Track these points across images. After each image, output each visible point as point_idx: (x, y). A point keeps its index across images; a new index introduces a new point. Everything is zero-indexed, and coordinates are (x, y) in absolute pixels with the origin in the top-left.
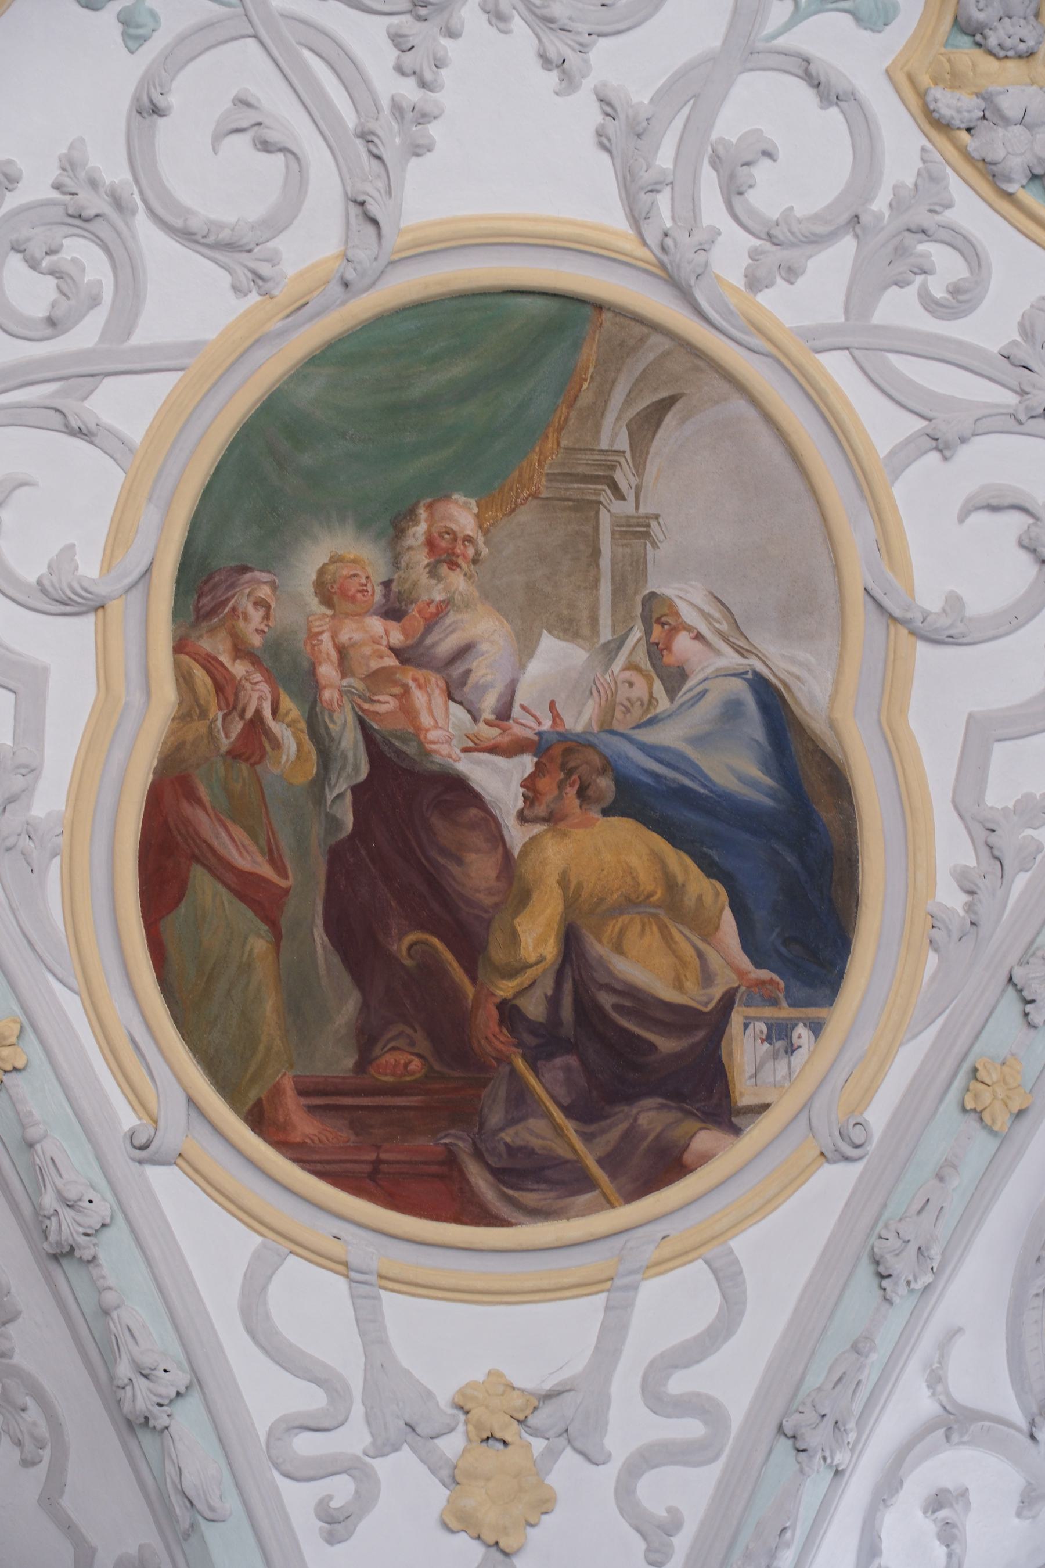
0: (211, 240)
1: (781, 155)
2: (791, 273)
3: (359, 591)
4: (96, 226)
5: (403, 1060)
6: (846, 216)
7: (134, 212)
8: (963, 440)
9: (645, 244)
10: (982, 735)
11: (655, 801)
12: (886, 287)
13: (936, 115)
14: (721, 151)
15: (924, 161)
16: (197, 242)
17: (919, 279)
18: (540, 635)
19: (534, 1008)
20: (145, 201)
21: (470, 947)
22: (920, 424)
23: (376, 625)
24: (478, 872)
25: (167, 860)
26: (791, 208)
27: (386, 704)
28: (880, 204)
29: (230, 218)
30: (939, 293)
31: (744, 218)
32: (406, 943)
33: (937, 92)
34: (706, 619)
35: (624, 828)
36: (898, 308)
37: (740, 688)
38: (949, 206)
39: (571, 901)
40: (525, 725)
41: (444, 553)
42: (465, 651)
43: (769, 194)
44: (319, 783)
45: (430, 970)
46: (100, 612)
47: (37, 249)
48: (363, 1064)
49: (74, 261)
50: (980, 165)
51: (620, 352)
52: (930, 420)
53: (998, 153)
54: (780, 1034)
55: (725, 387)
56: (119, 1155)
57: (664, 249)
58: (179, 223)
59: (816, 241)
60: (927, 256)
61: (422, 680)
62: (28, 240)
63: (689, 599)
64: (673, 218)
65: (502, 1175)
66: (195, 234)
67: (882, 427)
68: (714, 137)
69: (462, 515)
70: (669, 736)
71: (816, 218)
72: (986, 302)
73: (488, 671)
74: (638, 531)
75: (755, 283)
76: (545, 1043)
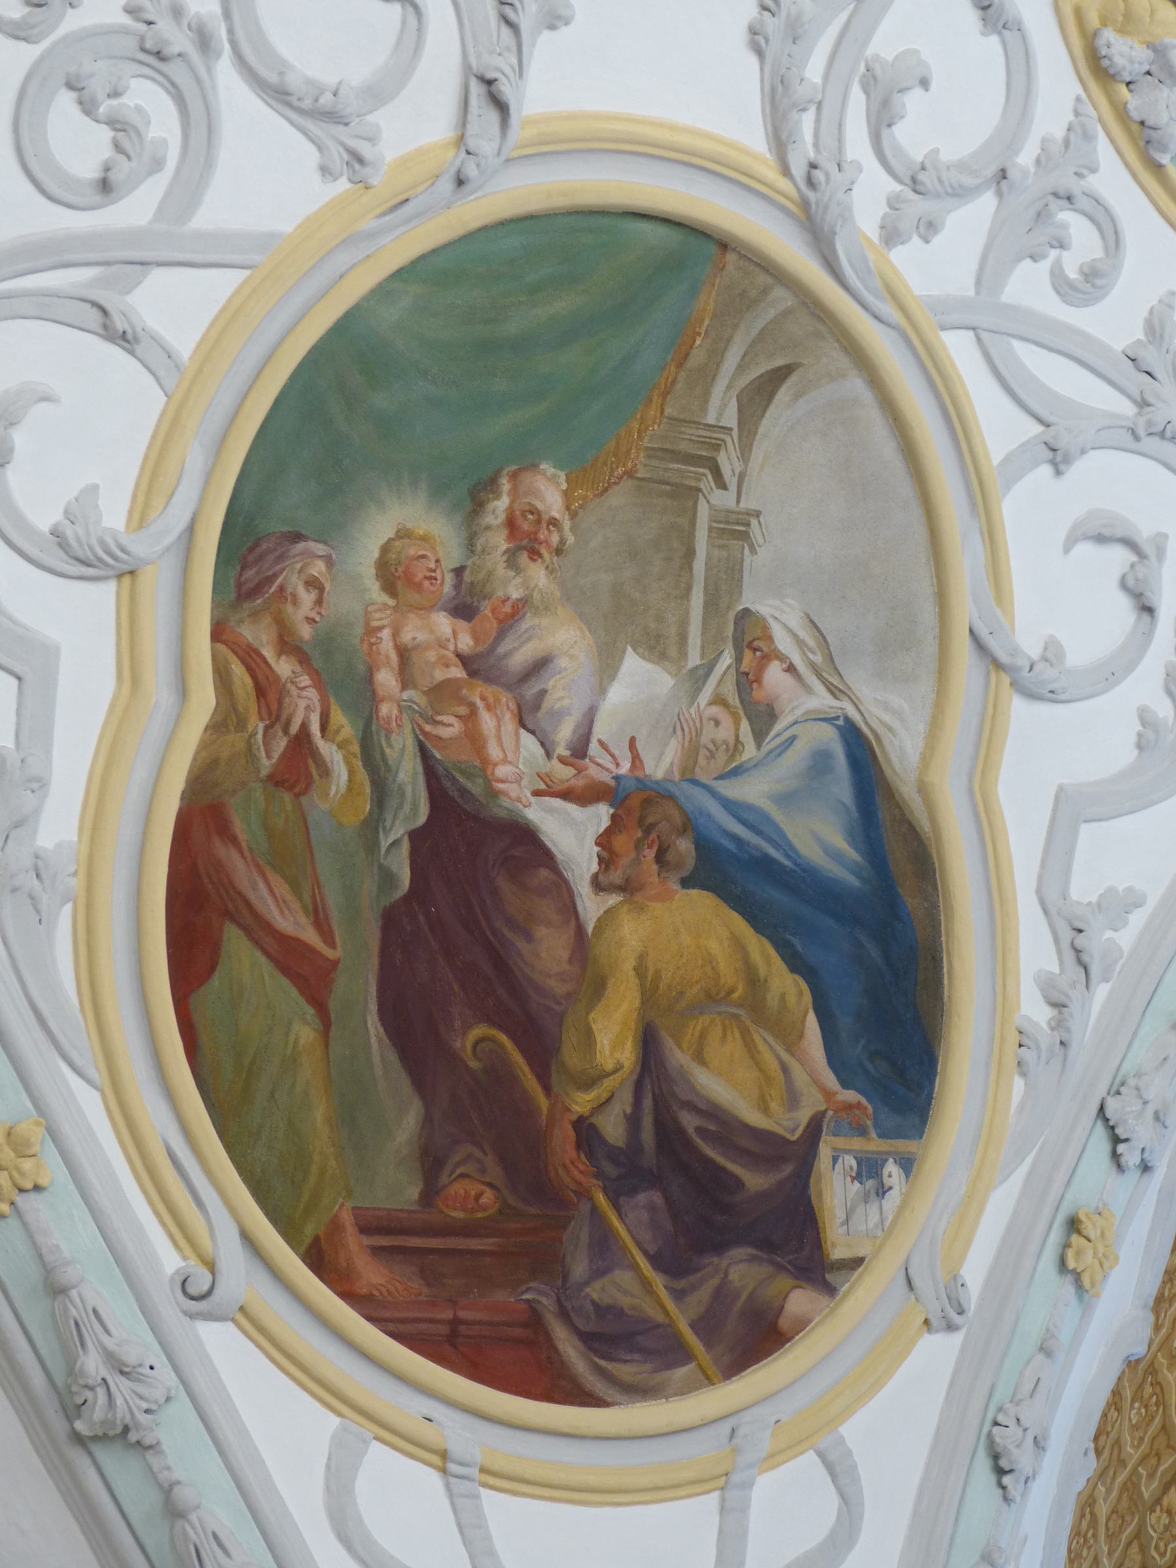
0: (307, 104)
1: (934, 86)
2: (929, 228)
3: (426, 578)
4: (174, 69)
5: (474, 1191)
6: (991, 170)
7: (219, 55)
8: (1083, 452)
9: (786, 171)
10: (1072, 810)
11: (737, 871)
12: (1020, 259)
13: (1105, 63)
14: (878, 71)
15: (1077, 114)
16: (289, 105)
17: (1053, 253)
18: (624, 652)
19: (613, 1128)
20: (233, 43)
21: (541, 1048)
22: (1038, 429)
23: (443, 623)
24: (547, 953)
25: (199, 915)
26: (936, 151)
27: (450, 728)
28: (1026, 158)
29: (330, 79)
30: (1073, 274)
31: (888, 153)
32: (473, 1038)
33: (1109, 35)
34: (800, 648)
35: (701, 905)
36: (1028, 286)
37: (829, 736)
38: (1093, 170)
39: (649, 994)
40: (604, 766)
41: (526, 535)
42: (540, 665)
43: (919, 131)
44: (372, 826)
45: (499, 1074)
46: (126, 580)
47: (97, 87)
48: (429, 1196)
49: (139, 109)
50: (1135, 127)
51: (739, 304)
52: (1048, 426)
53: (1158, 116)
54: (869, 1169)
55: (842, 361)
56: (169, 1306)
57: (811, 183)
58: (272, 78)
59: (961, 194)
60: (1064, 226)
61: (491, 700)
62: (91, 75)
63: (784, 618)
64: (816, 145)
65: (591, 1341)
66: (288, 94)
67: (1000, 427)
68: (869, 52)
69: (549, 492)
70: (753, 790)
71: (961, 166)
72: (1115, 292)
73: (565, 692)
74: (736, 530)
75: (891, 235)
76: (626, 1173)
